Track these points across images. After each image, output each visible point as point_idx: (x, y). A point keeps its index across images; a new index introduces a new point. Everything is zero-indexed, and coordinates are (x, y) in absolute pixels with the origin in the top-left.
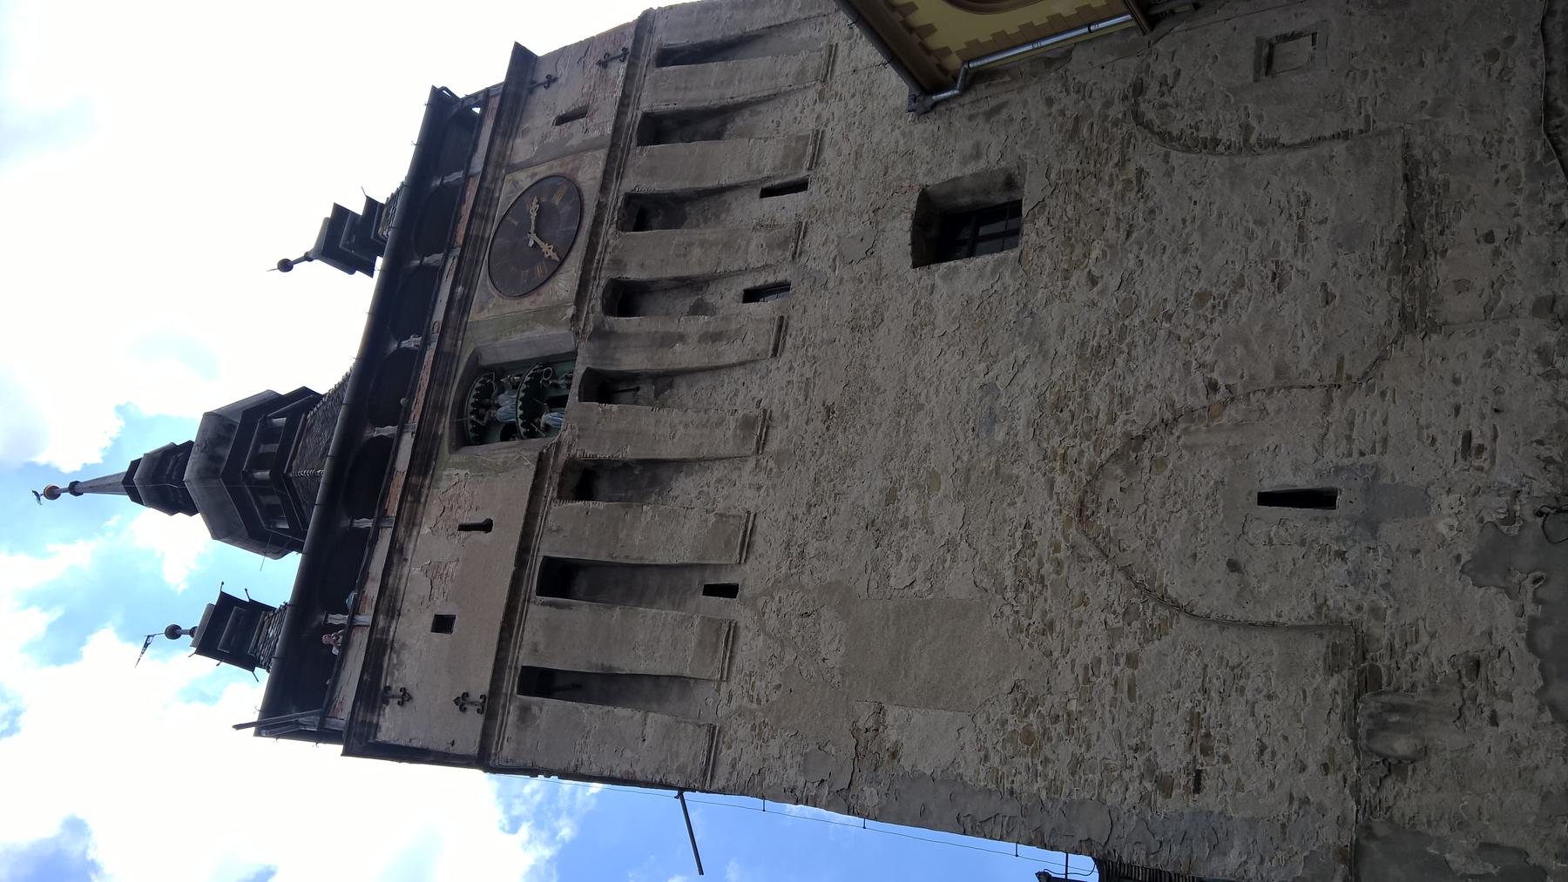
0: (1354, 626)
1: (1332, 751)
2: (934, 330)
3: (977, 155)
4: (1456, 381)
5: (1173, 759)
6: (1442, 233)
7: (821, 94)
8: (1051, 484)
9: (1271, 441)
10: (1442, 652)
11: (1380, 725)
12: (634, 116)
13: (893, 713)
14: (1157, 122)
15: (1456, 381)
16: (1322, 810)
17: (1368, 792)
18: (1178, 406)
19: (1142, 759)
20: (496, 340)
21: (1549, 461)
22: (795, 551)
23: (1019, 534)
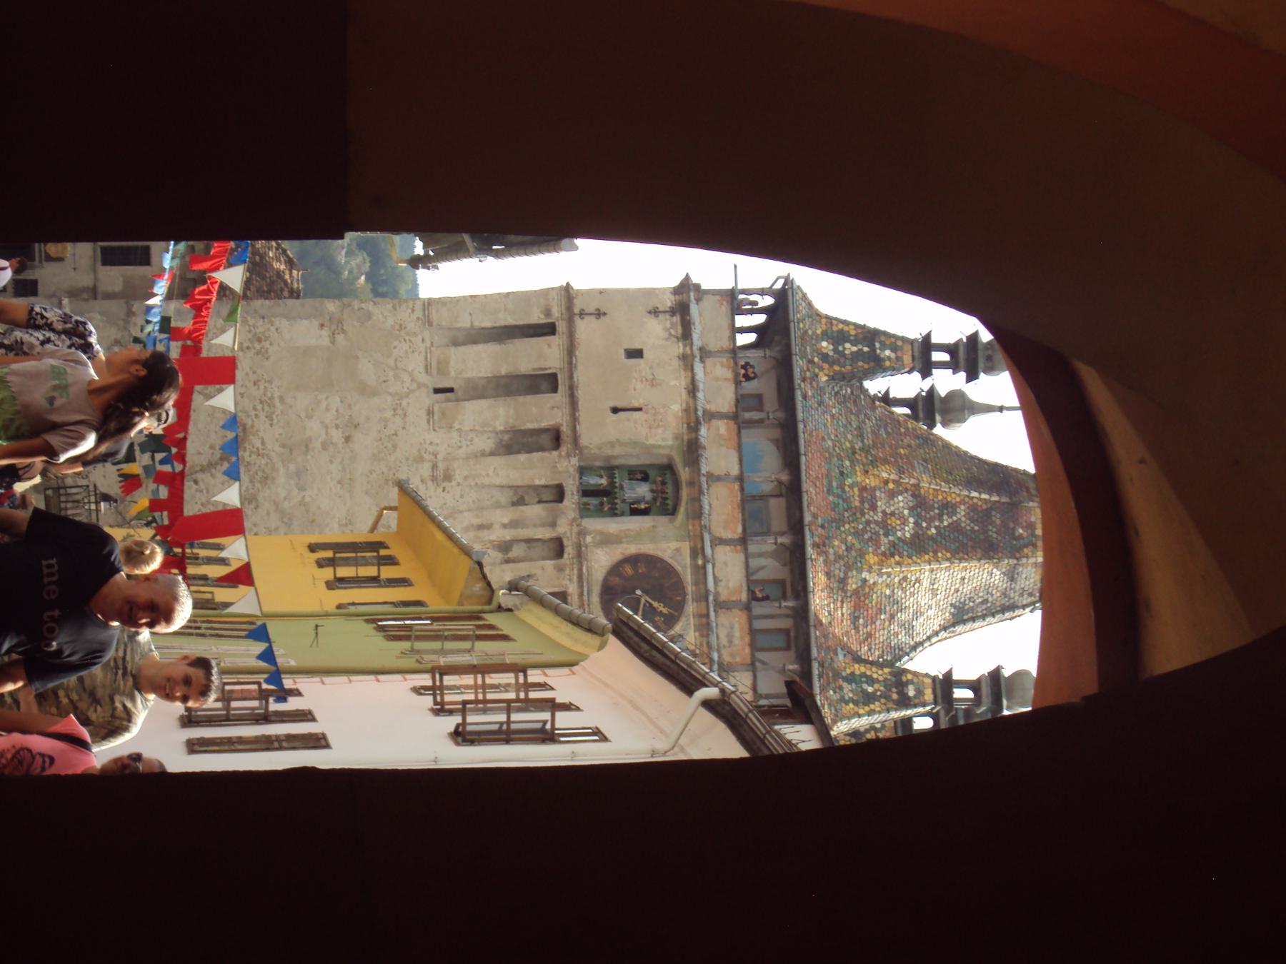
2: (339, 521)
8: (263, 443)
13: (326, 341)
15: (104, 477)
18: (209, 474)
20: (653, 526)
22: (399, 411)
23: (275, 421)
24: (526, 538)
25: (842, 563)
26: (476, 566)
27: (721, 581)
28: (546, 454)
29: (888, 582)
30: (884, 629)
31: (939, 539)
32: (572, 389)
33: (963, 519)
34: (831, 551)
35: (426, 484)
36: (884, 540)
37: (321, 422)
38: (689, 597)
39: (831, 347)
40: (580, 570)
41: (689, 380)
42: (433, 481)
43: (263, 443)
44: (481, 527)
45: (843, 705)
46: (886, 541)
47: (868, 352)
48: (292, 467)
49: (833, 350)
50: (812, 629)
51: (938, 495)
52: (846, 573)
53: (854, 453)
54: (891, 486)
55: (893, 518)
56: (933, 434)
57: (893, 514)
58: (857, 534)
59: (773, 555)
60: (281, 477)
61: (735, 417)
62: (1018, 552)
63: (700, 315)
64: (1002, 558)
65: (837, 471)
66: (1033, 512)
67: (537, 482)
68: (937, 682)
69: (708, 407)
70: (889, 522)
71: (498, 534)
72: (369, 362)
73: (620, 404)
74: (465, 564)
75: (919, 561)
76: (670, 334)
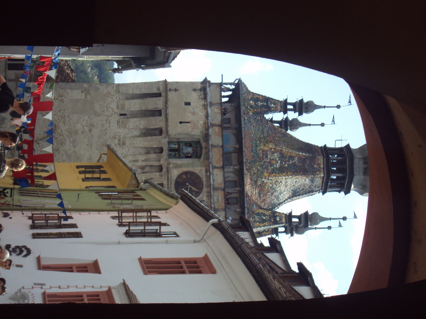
8: (62, 131)
13: (83, 97)
18: (43, 141)
20: (193, 162)
22: (108, 122)
23: (66, 124)
24: (150, 165)
25: (256, 175)
26: (134, 175)
27: (215, 181)
28: (157, 137)
29: (271, 182)
30: (269, 198)
31: (288, 168)
32: (166, 115)
33: (297, 162)
34: (252, 171)
35: (117, 146)
36: (270, 168)
37: (82, 125)
38: (204, 186)
39: (254, 103)
40: (168, 176)
41: (206, 113)
42: (119, 145)
43: (62, 131)
44: (135, 161)
45: (255, 223)
46: (271, 169)
47: (266, 105)
48: (71, 139)
49: (254, 104)
50: (245, 198)
51: (288, 153)
52: (257, 179)
53: (261, 139)
54: (273, 150)
55: (273, 161)
56: (287, 133)
57: (273, 159)
58: (261, 166)
59: (233, 172)
60: (68, 142)
61: (221, 126)
62: (315, 173)
63: (210, 91)
64: (309, 175)
65: (255, 144)
66: (320, 160)
67: (154, 146)
68: (287, 216)
69: (212, 122)
70: (272, 162)
71: (140, 164)
72: (98, 104)
73: (182, 121)
74: (130, 174)
75: (281, 175)
76: (200, 97)
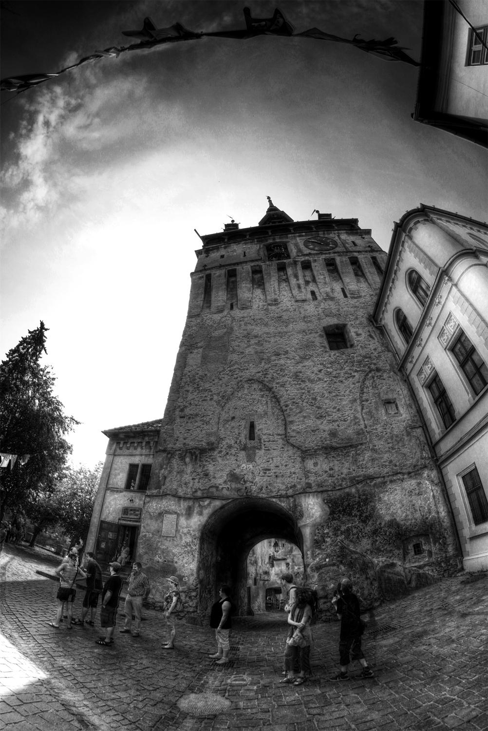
0: (217, 447)
1: (188, 445)
3: (358, 335)
4: (286, 466)
5: (188, 411)
6: (333, 457)
7: (372, 295)
8: (259, 372)
9: (269, 422)
10: (211, 468)
11: (192, 454)
12: (356, 254)
13: (201, 350)
14: (368, 377)
15: (286, 466)
16: (175, 444)
17: (178, 452)
19: (187, 404)
21: (261, 489)
22: (241, 319)
32: (234, 264)
43: (259, 372)
71: (301, 281)
